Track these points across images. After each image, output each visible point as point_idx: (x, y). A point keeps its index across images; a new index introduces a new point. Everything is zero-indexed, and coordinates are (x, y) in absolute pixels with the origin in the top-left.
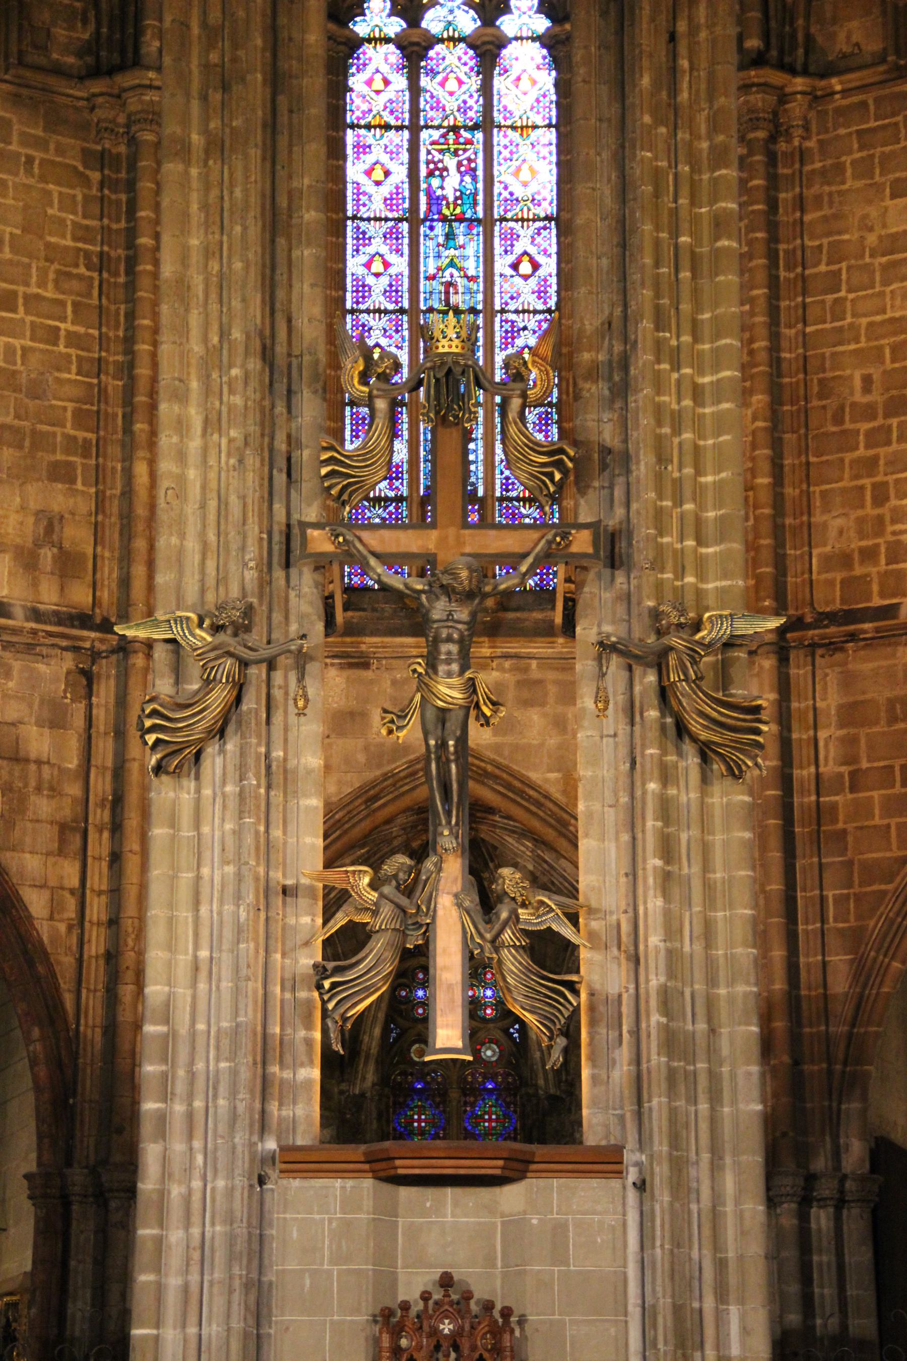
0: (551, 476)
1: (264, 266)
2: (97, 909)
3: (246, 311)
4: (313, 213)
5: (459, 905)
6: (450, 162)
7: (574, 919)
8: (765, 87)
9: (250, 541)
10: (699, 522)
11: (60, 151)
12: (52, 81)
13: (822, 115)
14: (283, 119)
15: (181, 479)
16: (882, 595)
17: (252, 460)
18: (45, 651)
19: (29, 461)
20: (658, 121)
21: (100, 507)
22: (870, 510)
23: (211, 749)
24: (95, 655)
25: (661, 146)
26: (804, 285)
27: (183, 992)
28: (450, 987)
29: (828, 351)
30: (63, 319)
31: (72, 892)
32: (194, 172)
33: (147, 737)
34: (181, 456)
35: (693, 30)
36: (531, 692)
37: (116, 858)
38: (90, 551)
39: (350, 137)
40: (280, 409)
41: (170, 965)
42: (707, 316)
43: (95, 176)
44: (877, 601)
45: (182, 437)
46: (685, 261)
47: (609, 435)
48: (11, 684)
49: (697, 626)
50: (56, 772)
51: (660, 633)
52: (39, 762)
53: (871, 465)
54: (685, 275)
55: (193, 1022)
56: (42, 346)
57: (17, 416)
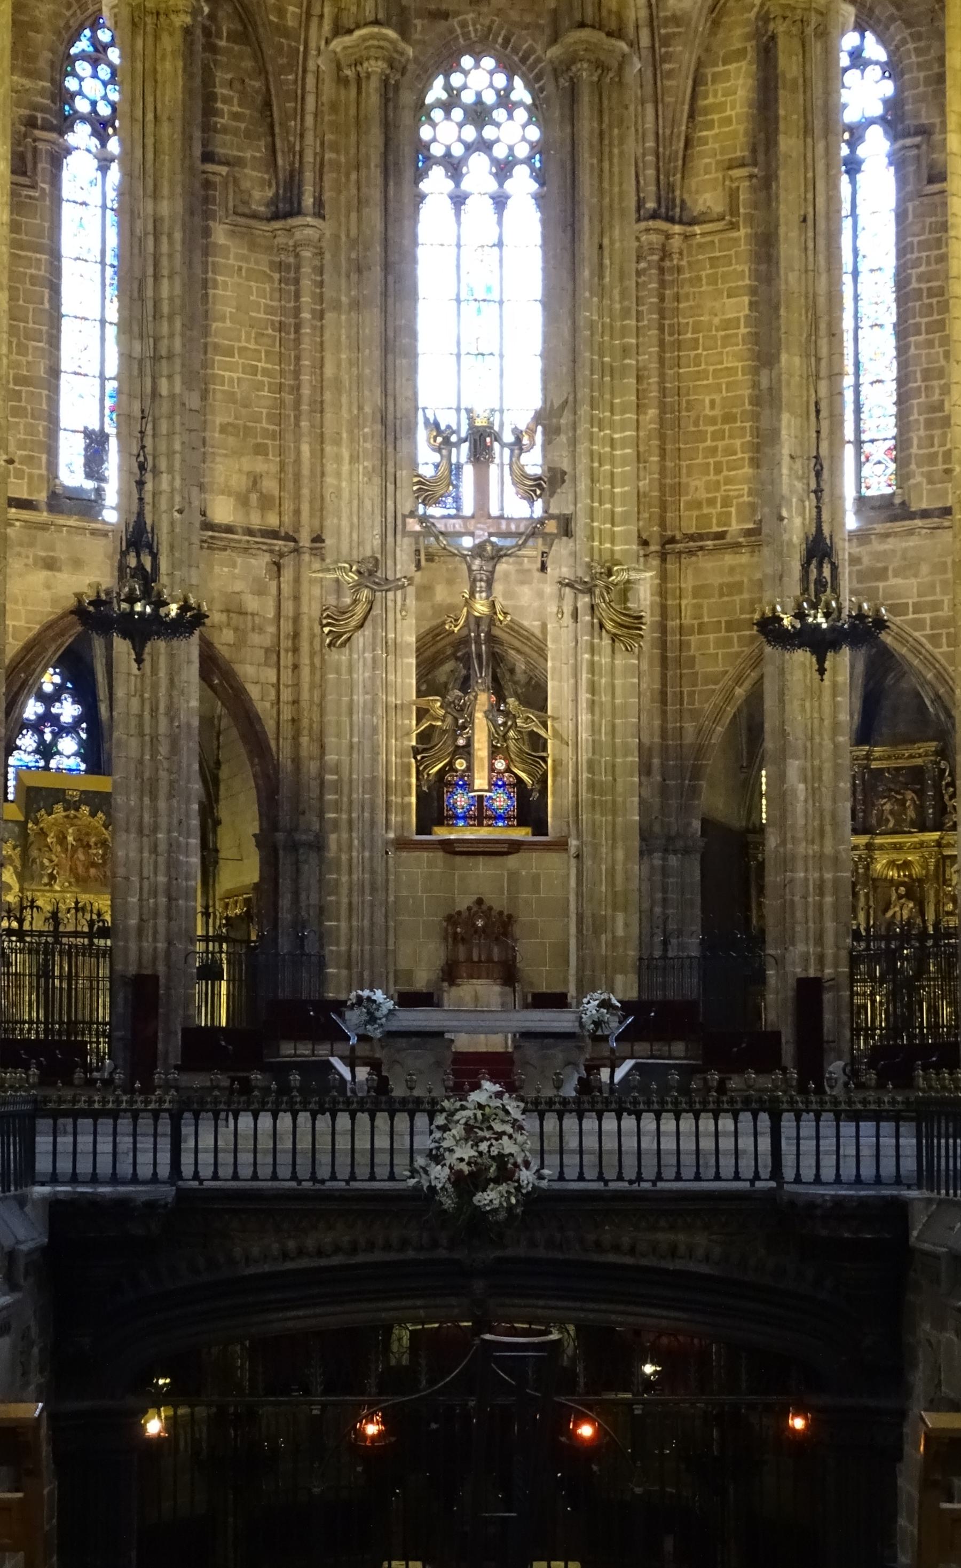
2: (286, 695)
8: (657, 231)
11: (257, 263)
13: (690, 246)
15: (339, 489)
16: (718, 525)
17: (377, 480)
21: (282, 469)
22: (712, 477)
24: (281, 555)
25: (595, 309)
26: (679, 345)
29: (691, 384)
34: (338, 475)
35: (612, 242)
37: (296, 667)
38: (276, 493)
40: (390, 449)
43: (276, 276)
44: (716, 529)
46: (607, 372)
47: (565, 465)
49: (610, 574)
52: (253, 614)
53: (713, 451)
54: (607, 379)
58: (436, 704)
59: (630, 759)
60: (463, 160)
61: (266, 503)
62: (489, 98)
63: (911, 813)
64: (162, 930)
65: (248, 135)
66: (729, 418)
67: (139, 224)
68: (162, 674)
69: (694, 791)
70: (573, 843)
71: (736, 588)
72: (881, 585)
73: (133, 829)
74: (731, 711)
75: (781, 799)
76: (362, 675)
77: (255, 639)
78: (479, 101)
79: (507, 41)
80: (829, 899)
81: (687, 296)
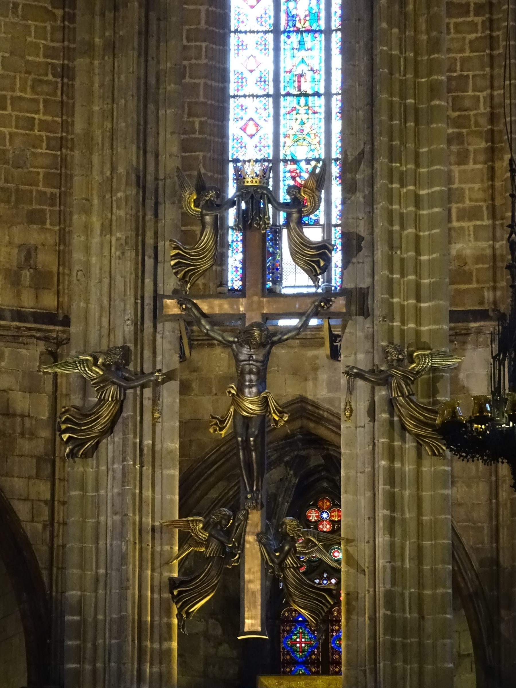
0: (318, 263)
1: (139, 124)
3: (128, 155)
4: (172, 86)
5: (260, 541)
9: (128, 307)
10: (418, 286)
14: (153, 27)
15: (87, 264)
17: (130, 254)
18: (25, 340)
19: (14, 211)
20: (391, 26)
25: (395, 41)
28: (253, 593)
30: (37, 112)
31: (46, 502)
32: (96, 63)
33: (63, 436)
34: (87, 249)
38: (55, 270)
40: (149, 216)
41: (81, 578)
42: (425, 150)
43: (59, 13)
45: (87, 236)
46: (411, 116)
47: (362, 230)
48: (3, 364)
50: (34, 422)
52: (22, 416)
54: (411, 124)
55: (96, 614)
56: (23, 131)
57: (6, 181)
59: (440, 591)
76: (111, 490)
77: (25, 446)
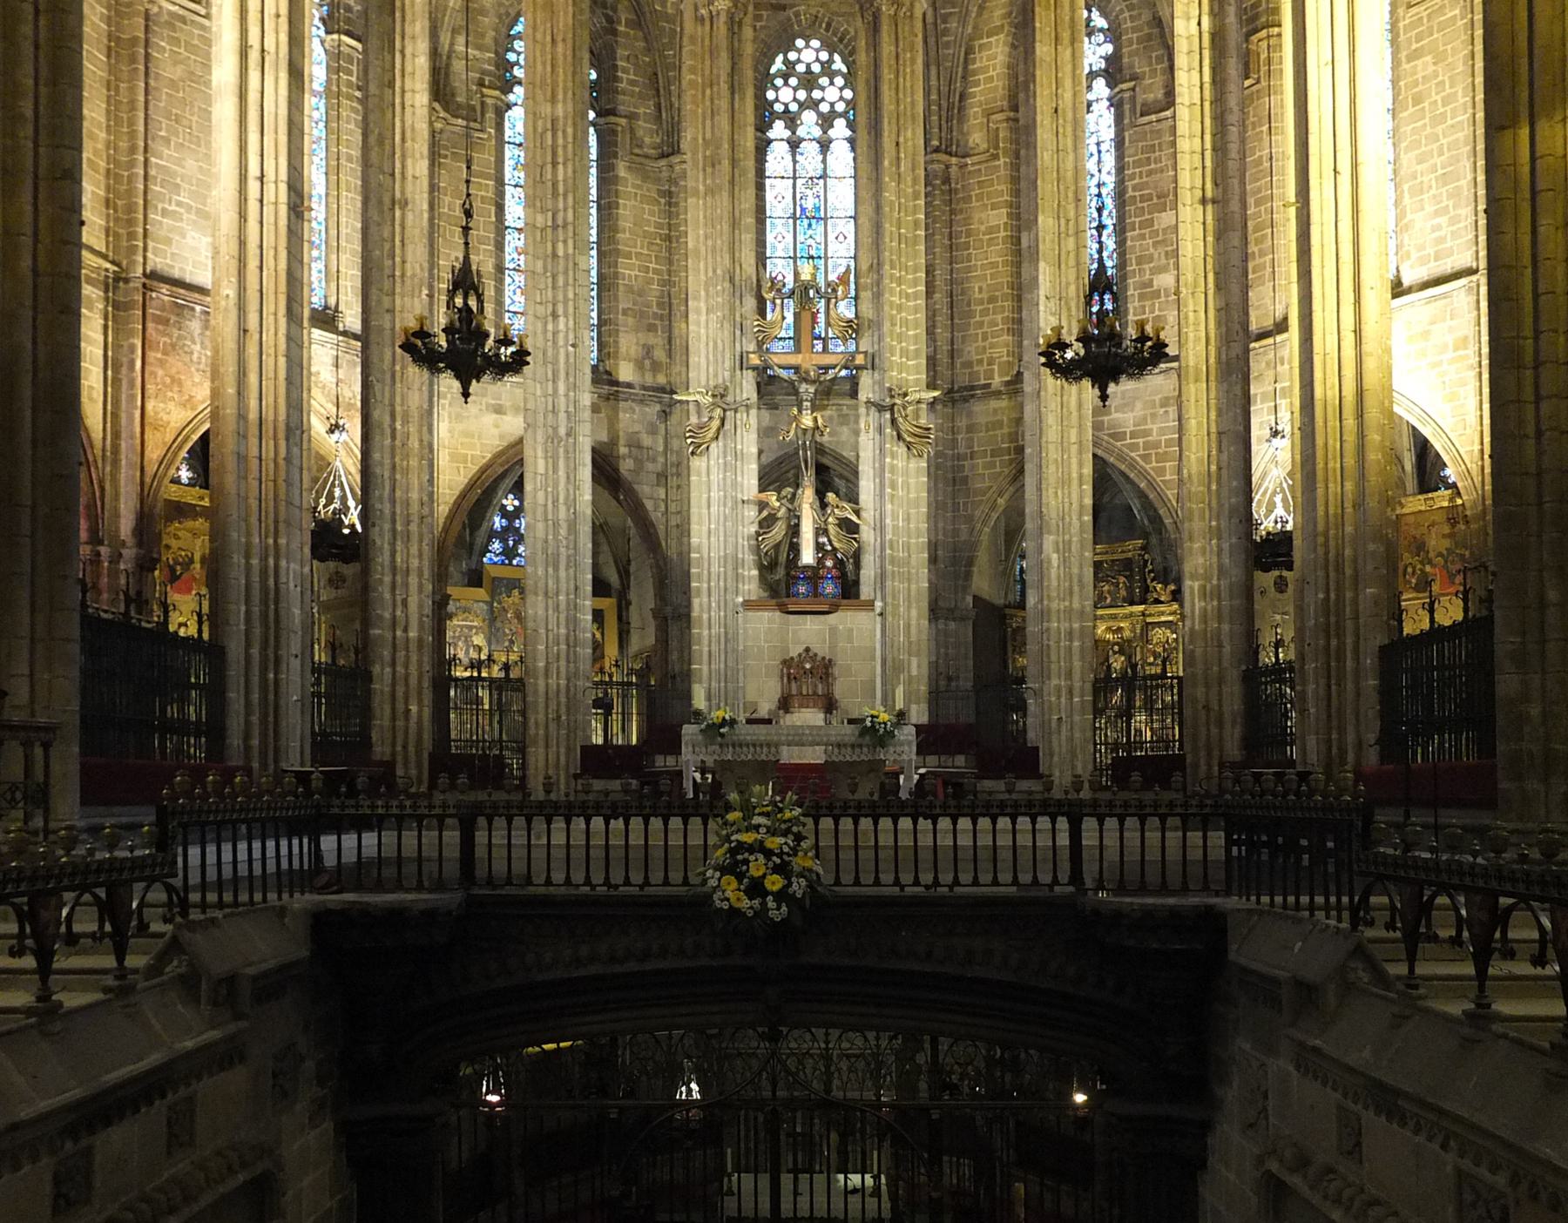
6: (809, 192)
7: (857, 513)
12: (646, 161)
22: (980, 343)
23: (713, 445)
27: (705, 541)
34: (698, 324)
36: (844, 419)
39: (768, 182)
49: (905, 395)
51: (892, 397)
53: (981, 324)
58: (772, 498)
60: (799, 113)
61: (656, 367)
62: (816, 68)
63: (1123, 593)
64: (563, 670)
65: (641, 96)
66: (992, 300)
67: (540, 123)
68: (562, 473)
69: (968, 575)
70: (878, 604)
71: (1000, 424)
72: (1106, 418)
73: (541, 593)
74: (995, 516)
75: (1041, 567)
77: (650, 466)
78: (809, 71)
79: (829, 25)
80: (1076, 644)
81: (961, 211)
